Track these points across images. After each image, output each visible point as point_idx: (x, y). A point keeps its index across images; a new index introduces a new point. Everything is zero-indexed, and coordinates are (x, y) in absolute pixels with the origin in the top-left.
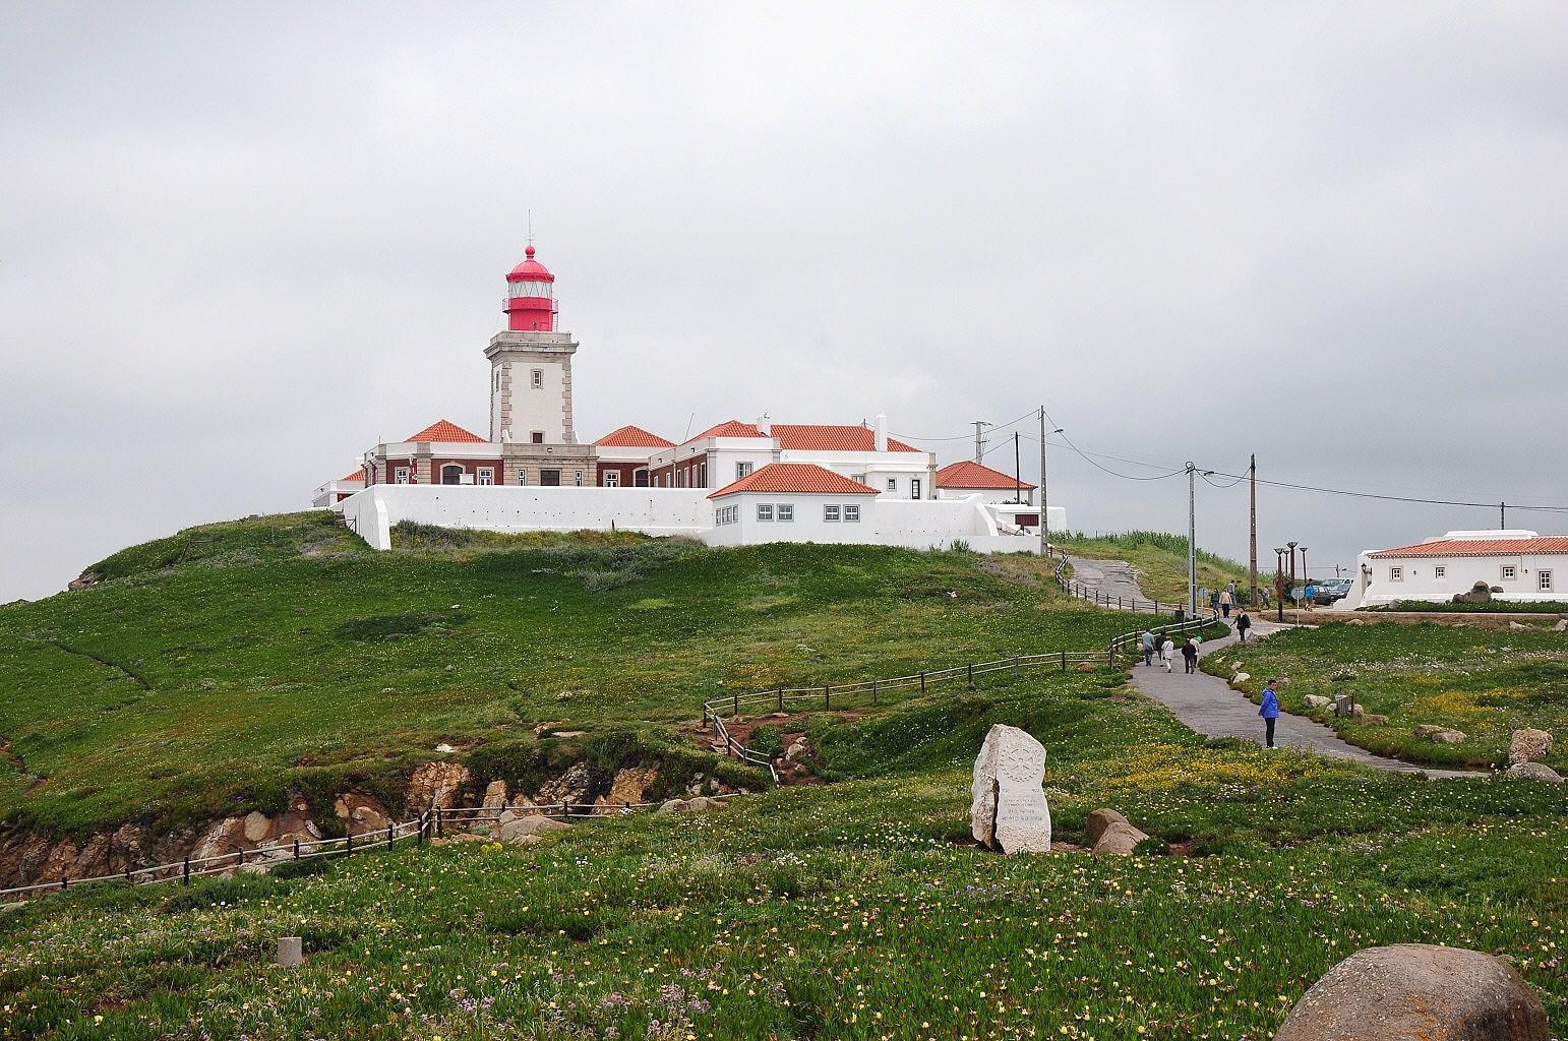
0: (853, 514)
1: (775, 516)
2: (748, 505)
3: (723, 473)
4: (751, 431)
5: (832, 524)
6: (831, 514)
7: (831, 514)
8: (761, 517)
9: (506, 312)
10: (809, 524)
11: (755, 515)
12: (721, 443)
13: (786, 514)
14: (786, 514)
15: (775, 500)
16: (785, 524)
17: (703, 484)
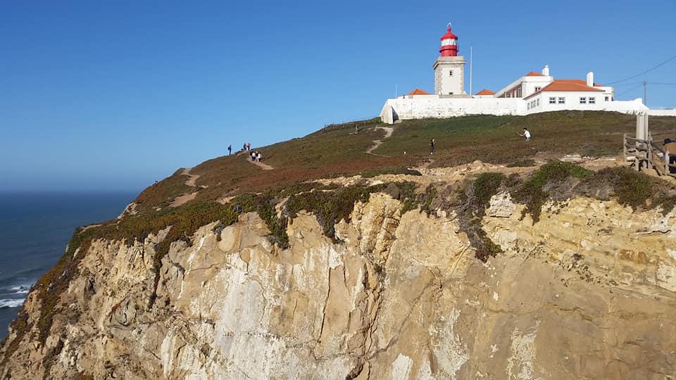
0: (592, 101)
1: (557, 101)
2: (545, 96)
3: (528, 89)
4: (540, 74)
5: (583, 104)
6: (583, 101)
7: (583, 101)
8: (551, 102)
9: (441, 52)
10: (572, 101)
11: (548, 100)
12: (528, 79)
13: (562, 101)
14: (562, 101)
15: (557, 95)
16: (561, 105)
17: (519, 95)
